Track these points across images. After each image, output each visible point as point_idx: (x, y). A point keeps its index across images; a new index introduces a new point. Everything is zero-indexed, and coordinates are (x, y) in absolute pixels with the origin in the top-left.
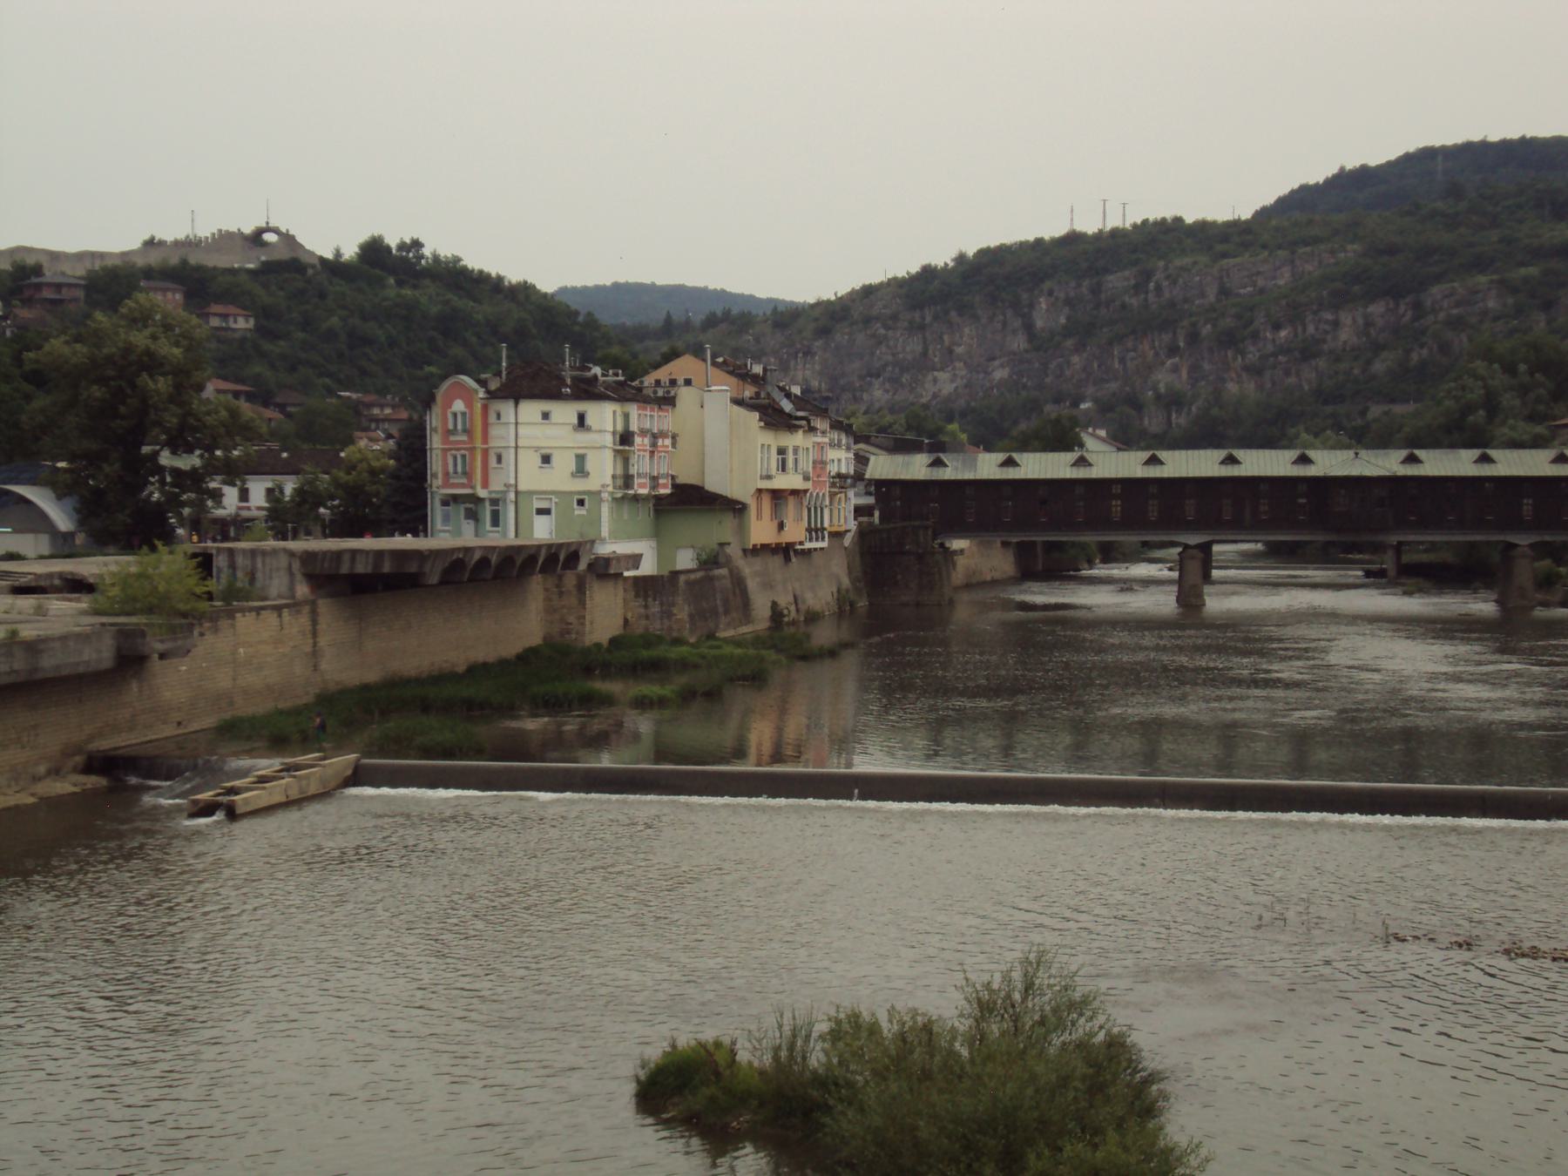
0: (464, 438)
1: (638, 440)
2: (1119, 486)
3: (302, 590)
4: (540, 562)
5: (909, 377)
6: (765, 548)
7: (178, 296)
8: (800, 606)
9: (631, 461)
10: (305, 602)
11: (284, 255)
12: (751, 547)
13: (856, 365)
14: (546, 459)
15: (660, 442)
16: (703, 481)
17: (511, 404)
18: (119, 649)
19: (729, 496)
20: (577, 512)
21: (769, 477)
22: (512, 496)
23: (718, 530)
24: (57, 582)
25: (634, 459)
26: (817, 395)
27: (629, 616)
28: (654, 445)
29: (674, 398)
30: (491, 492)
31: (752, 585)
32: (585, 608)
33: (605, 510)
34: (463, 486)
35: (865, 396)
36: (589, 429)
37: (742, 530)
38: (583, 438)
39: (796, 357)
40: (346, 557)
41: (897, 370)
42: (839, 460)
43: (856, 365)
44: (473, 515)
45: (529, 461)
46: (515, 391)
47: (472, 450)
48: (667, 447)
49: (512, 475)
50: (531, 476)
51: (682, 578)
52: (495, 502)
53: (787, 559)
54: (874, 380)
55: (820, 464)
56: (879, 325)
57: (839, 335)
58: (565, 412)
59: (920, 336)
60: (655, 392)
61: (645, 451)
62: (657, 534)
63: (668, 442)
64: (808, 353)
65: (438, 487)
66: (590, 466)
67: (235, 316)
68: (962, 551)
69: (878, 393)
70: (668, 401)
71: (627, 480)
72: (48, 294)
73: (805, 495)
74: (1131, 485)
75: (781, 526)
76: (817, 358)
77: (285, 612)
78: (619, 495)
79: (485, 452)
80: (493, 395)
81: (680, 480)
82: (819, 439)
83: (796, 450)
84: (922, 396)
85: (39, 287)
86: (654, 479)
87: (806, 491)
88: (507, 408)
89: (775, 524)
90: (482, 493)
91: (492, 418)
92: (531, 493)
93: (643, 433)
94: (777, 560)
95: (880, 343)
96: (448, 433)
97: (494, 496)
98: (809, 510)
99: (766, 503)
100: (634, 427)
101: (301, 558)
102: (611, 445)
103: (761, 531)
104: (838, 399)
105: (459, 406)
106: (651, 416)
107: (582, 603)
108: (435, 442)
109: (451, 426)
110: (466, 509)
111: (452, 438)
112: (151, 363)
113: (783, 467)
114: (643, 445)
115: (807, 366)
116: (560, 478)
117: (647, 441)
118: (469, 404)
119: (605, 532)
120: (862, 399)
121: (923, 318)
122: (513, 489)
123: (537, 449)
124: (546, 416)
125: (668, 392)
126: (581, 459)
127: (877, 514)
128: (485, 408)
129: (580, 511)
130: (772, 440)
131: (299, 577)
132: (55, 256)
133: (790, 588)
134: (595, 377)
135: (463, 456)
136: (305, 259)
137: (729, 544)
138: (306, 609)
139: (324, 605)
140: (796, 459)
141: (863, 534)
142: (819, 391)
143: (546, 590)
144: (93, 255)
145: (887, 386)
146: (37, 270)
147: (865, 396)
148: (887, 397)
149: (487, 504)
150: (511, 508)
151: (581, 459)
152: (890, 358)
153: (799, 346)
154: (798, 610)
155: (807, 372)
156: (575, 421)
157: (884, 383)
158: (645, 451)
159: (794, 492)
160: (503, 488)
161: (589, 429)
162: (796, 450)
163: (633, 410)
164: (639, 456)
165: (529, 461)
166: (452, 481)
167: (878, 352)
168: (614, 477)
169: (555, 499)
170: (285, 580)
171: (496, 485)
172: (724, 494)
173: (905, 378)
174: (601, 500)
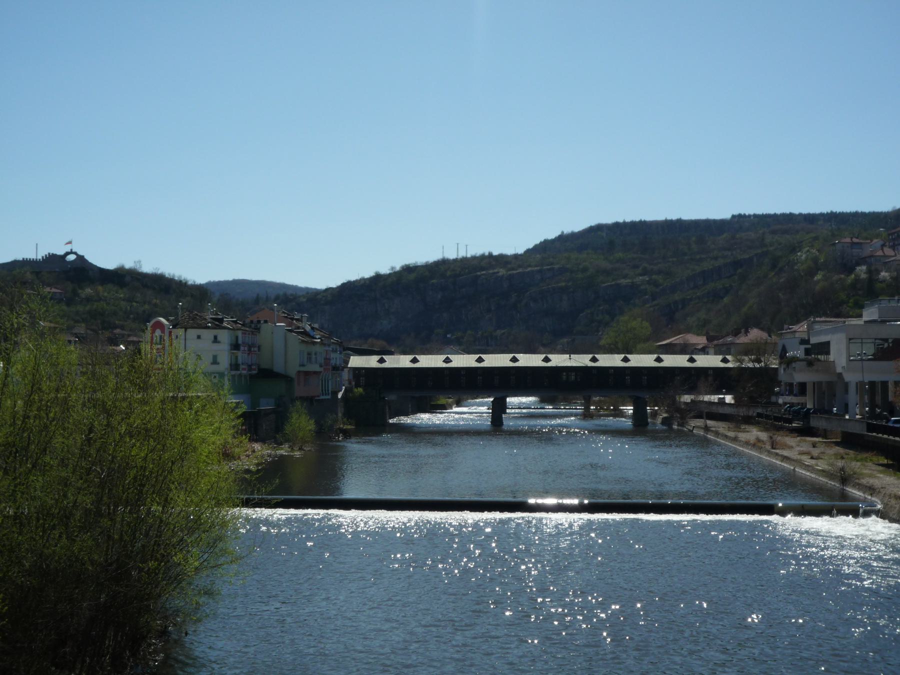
1: (242, 348)
15: (252, 349)
21: (303, 365)
28: (250, 350)
36: (219, 342)
38: (216, 346)
42: (336, 358)
55: (327, 360)
58: (208, 335)
63: (256, 349)
66: (219, 359)
82: (327, 348)
83: (316, 354)
86: (250, 366)
87: (321, 372)
88: (180, 332)
98: (322, 381)
113: (309, 359)
117: (246, 349)
125: (257, 326)
126: (215, 357)
140: (316, 358)
151: (215, 357)
156: (213, 338)
159: (315, 373)
161: (219, 342)
162: (316, 354)
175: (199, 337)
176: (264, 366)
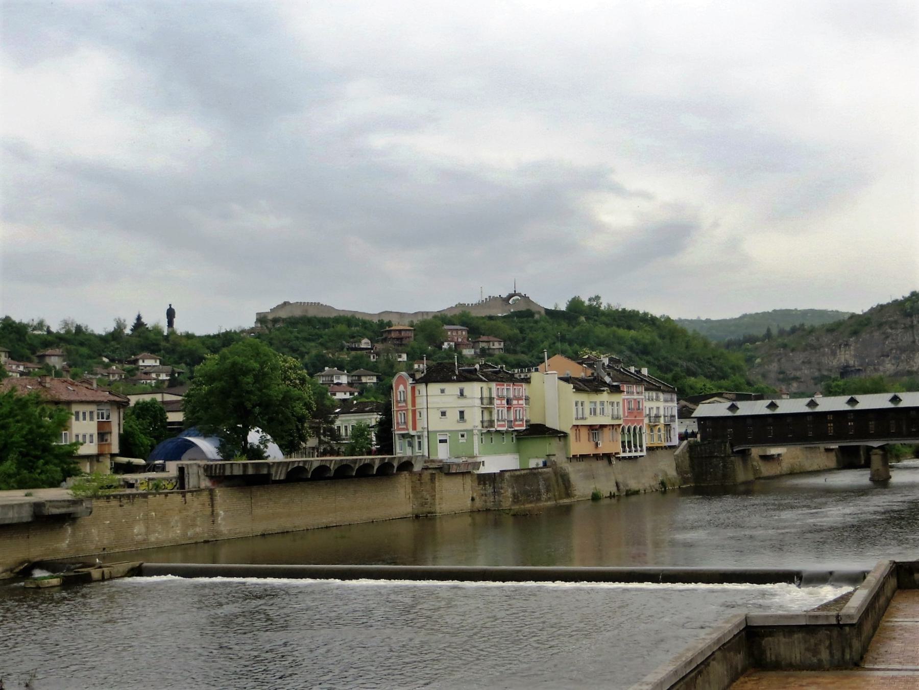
0: (404, 404)
1: (496, 402)
2: (831, 416)
3: (205, 483)
4: (376, 468)
5: (905, 356)
6: (583, 457)
7: (464, 333)
8: (621, 487)
9: (493, 413)
10: (207, 489)
11: (523, 307)
12: (571, 456)
13: (875, 351)
14: (443, 414)
15: (515, 402)
16: (545, 422)
17: (424, 386)
18: (34, 513)
19: (558, 429)
20: (460, 441)
21: (583, 418)
22: (426, 433)
23: (552, 446)
24: (122, 483)
25: (495, 412)
26: (853, 369)
27: (475, 495)
29: (530, 378)
30: (417, 432)
31: (574, 478)
32: (435, 491)
33: (476, 439)
34: (403, 429)
35: (881, 368)
36: (465, 397)
37: (566, 447)
38: (463, 402)
39: (840, 348)
40: (228, 468)
41: (898, 352)
42: (658, 408)
43: (875, 351)
44: (411, 445)
45: (435, 416)
46: (427, 380)
47: (407, 410)
48: (522, 405)
49: (426, 422)
50: (435, 423)
51: (507, 474)
52: (419, 437)
53: (610, 462)
54: (885, 358)
55: (635, 410)
56: (887, 327)
57: (864, 334)
58: (452, 389)
59: (911, 332)
60: (520, 376)
61: (504, 407)
62: (518, 451)
64: (847, 345)
65: (397, 432)
67: (493, 341)
68: (779, 455)
69: (889, 366)
70: (527, 381)
71: (491, 423)
72: (393, 335)
73: (619, 427)
74: (838, 415)
75: (597, 444)
76: (852, 348)
77: (188, 495)
78: (485, 431)
79: (414, 412)
80: (417, 381)
81: (533, 422)
83: (602, 403)
84: (913, 366)
85: (390, 331)
87: (619, 425)
88: (422, 387)
89: (593, 444)
90: (412, 433)
91: (417, 392)
92: (436, 432)
93: (501, 398)
94: (601, 465)
95: (887, 337)
96: (398, 402)
97: (418, 434)
99: (584, 433)
100: (494, 395)
101: (204, 468)
102: (480, 405)
103: (580, 446)
104: (865, 370)
105: (401, 388)
106: (507, 389)
107: (434, 489)
108: (395, 408)
109: (399, 399)
110: (408, 441)
111: (400, 405)
112: (246, 372)
114: (501, 404)
115: (847, 352)
116: (451, 423)
117: (504, 402)
118: (405, 387)
119: (476, 452)
120: (879, 370)
121: (912, 322)
122: (426, 430)
123: (438, 408)
124: (443, 391)
125: (526, 375)
126: (462, 413)
127: (699, 436)
128: (413, 389)
129: (462, 440)
130: (585, 398)
131: (202, 477)
132: (401, 315)
133: (613, 478)
134: (476, 369)
135: (404, 414)
136: (534, 309)
137: (554, 455)
138: (206, 493)
139: (219, 492)
141: (691, 448)
142: (854, 366)
143: (412, 482)
144: (423, 313)
145: (893, 361)
146: (389, 324)
147: (881, 368)
148: (893, 368)
149: (416, 438)
150: (426, 440)
151: (462, 413)
152: (894, 345)
153: (841, 341)
154: (618, 489)
155: (846, 356)
157: (890, 360)
158: (504, 407)
160: (421, 430)
161: (465, 397)
162: (602, 403)
163: (493, 385)
164: (498, 411)
165: (435, 416)
166: (400, 427)
167: (887, 342)
168: (482, 422)
169: (448, 435)
170: (196, 479)
171: (419, 428)
172: (556, 428)
173: (903, 356)
174: (473, 435)
175: (462, 394)
176: (535, 421)
